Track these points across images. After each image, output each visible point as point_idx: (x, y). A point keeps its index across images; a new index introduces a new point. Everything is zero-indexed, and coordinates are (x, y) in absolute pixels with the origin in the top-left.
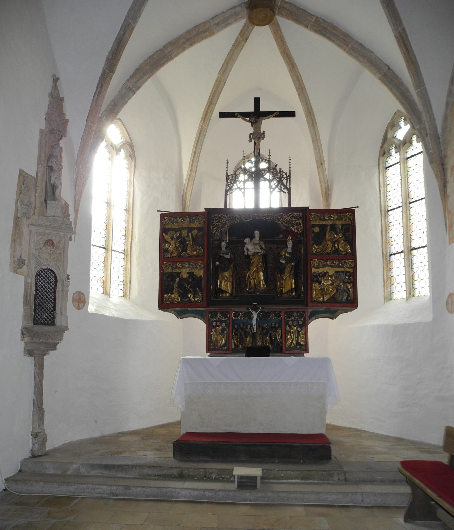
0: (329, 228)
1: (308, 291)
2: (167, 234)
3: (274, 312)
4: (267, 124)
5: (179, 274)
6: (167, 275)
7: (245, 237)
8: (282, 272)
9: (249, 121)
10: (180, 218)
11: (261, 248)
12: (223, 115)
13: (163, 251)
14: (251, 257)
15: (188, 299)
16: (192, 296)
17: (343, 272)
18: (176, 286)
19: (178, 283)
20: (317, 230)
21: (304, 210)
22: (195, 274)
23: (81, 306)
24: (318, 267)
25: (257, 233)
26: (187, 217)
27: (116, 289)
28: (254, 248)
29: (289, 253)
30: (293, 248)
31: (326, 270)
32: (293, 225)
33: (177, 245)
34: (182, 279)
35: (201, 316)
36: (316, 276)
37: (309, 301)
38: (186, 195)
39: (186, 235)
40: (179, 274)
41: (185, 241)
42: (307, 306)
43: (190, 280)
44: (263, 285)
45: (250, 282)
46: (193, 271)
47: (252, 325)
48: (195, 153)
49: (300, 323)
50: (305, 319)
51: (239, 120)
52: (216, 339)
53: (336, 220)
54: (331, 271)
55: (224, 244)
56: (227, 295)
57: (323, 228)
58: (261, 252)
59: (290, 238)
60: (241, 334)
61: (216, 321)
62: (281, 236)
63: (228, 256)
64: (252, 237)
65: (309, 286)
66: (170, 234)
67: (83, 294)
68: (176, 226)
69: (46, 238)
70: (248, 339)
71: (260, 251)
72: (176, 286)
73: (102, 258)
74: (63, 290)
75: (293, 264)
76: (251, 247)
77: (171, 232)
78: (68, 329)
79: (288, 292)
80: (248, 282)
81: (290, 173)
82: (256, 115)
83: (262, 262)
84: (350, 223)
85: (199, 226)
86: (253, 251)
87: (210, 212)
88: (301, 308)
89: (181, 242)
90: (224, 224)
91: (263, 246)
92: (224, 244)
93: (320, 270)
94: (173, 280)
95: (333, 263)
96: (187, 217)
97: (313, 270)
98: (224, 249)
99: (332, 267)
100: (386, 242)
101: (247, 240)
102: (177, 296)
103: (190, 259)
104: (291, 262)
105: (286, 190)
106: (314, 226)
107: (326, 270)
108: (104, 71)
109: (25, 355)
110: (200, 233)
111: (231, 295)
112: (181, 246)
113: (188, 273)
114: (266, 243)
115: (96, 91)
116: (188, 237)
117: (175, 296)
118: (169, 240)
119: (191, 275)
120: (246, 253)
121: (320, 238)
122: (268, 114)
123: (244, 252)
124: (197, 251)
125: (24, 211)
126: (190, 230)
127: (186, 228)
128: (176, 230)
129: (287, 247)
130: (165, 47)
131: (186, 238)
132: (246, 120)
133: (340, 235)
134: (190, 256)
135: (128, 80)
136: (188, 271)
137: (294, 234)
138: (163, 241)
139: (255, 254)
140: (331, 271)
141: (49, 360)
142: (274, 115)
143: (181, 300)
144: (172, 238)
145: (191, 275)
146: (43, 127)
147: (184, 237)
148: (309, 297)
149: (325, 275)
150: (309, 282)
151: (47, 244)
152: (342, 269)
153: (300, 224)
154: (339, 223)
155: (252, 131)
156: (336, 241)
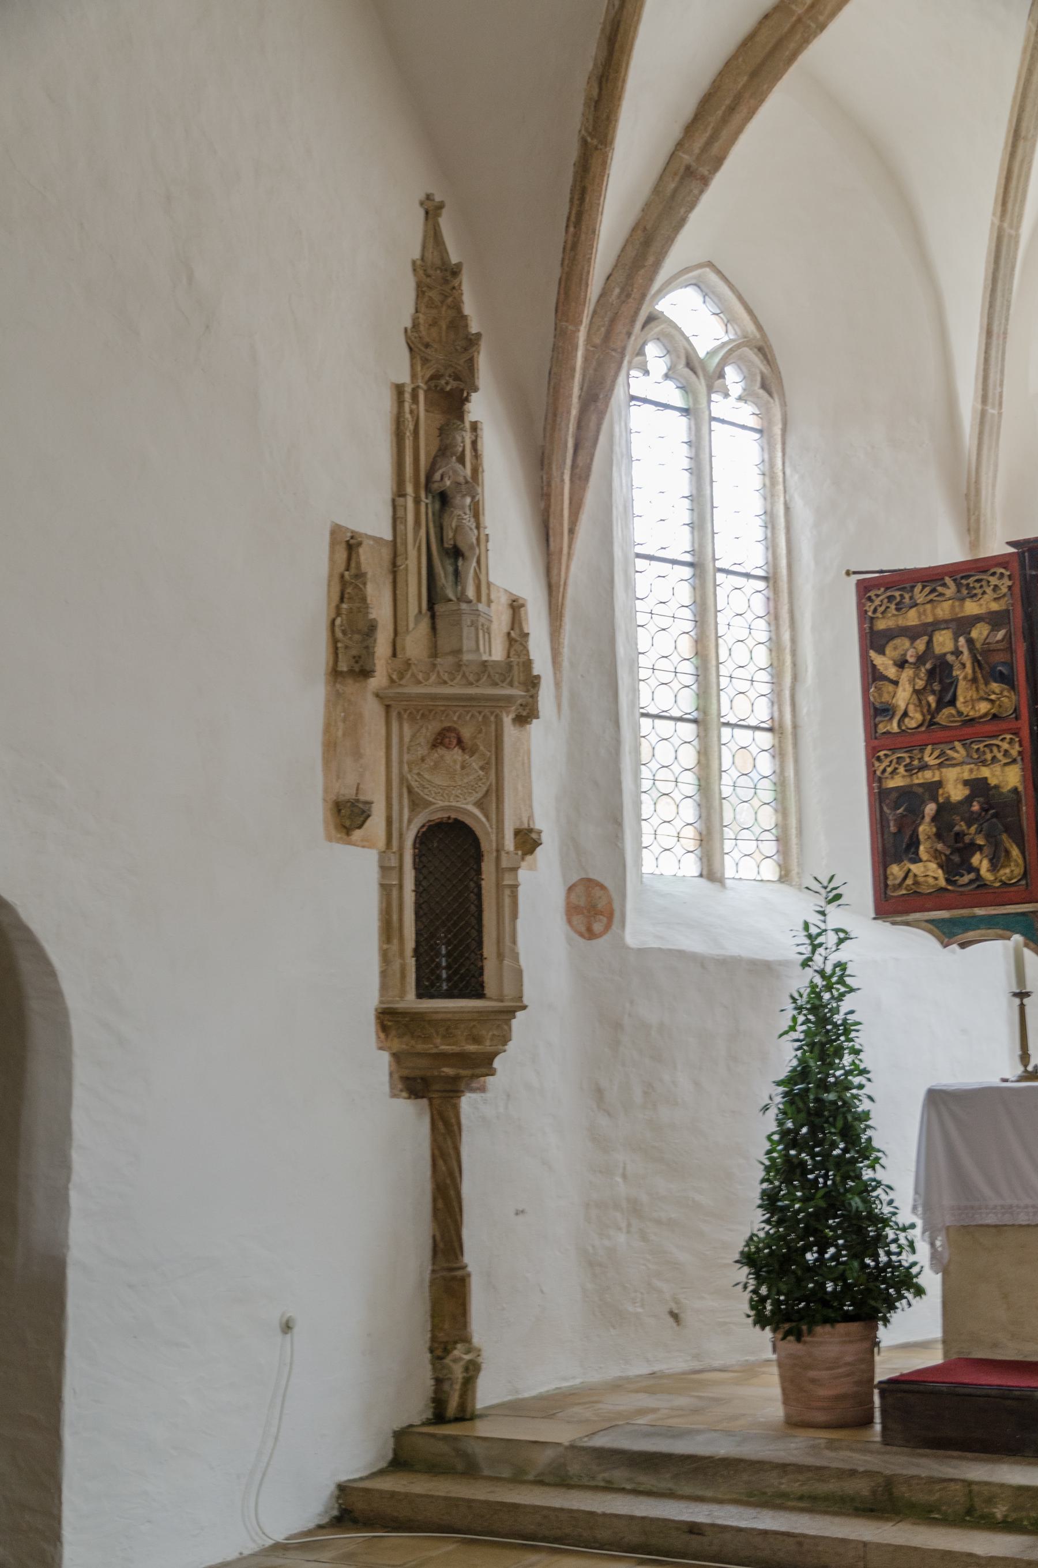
2: (881, 651)
5: (933, 789)
6: (894, 795)
10: (924, 587)
13: (876, 712)
15: (972, 876)
16: (985, 865)
18: (925, 829)
19: (934, 819)
22: (993, 782)
23: (597, 927)
26: (947, 580)
27: (749, 861)
34: (945, 809)
38: (978, 491)
40: (933, 789)
41: (950, 667)
43: (976, 807)
46: (985, 772)
48: (989, 333)
66: (895, 648)
67: (603, 887)
68: (912, 618)
69: (433, 727)
72: (925, 829)
73: (689, 756)
77: (897, 641)
78: (524, 1008)
85: (995, 607)
89: (931, 673)
94: (915, 814)
96: (947, 580)
102: (933, 866)
108: (584, 143)
109: (394, 1096)
110: (1000, 635)
112: (936, 687)
113: (966, 783)
115: (570, 213)
116: (957, 653)
117: (928, 871)
118: (891, 672)
119: (978, 787)
124: (992, 701)
125: (354, 652)
126: (962, 626)
127: (946, 621)
128: (912, 633)
131: (950, 658)
134: (971, 721)
135: (680, 145)
136: (966, 776)
138: (871, 676)
141: (468, 1103)
143: (947, 880)
144: (901, 664)
145: (978, 787)
146: (404, 377)
147: (945, 654)
151: (441, 743)
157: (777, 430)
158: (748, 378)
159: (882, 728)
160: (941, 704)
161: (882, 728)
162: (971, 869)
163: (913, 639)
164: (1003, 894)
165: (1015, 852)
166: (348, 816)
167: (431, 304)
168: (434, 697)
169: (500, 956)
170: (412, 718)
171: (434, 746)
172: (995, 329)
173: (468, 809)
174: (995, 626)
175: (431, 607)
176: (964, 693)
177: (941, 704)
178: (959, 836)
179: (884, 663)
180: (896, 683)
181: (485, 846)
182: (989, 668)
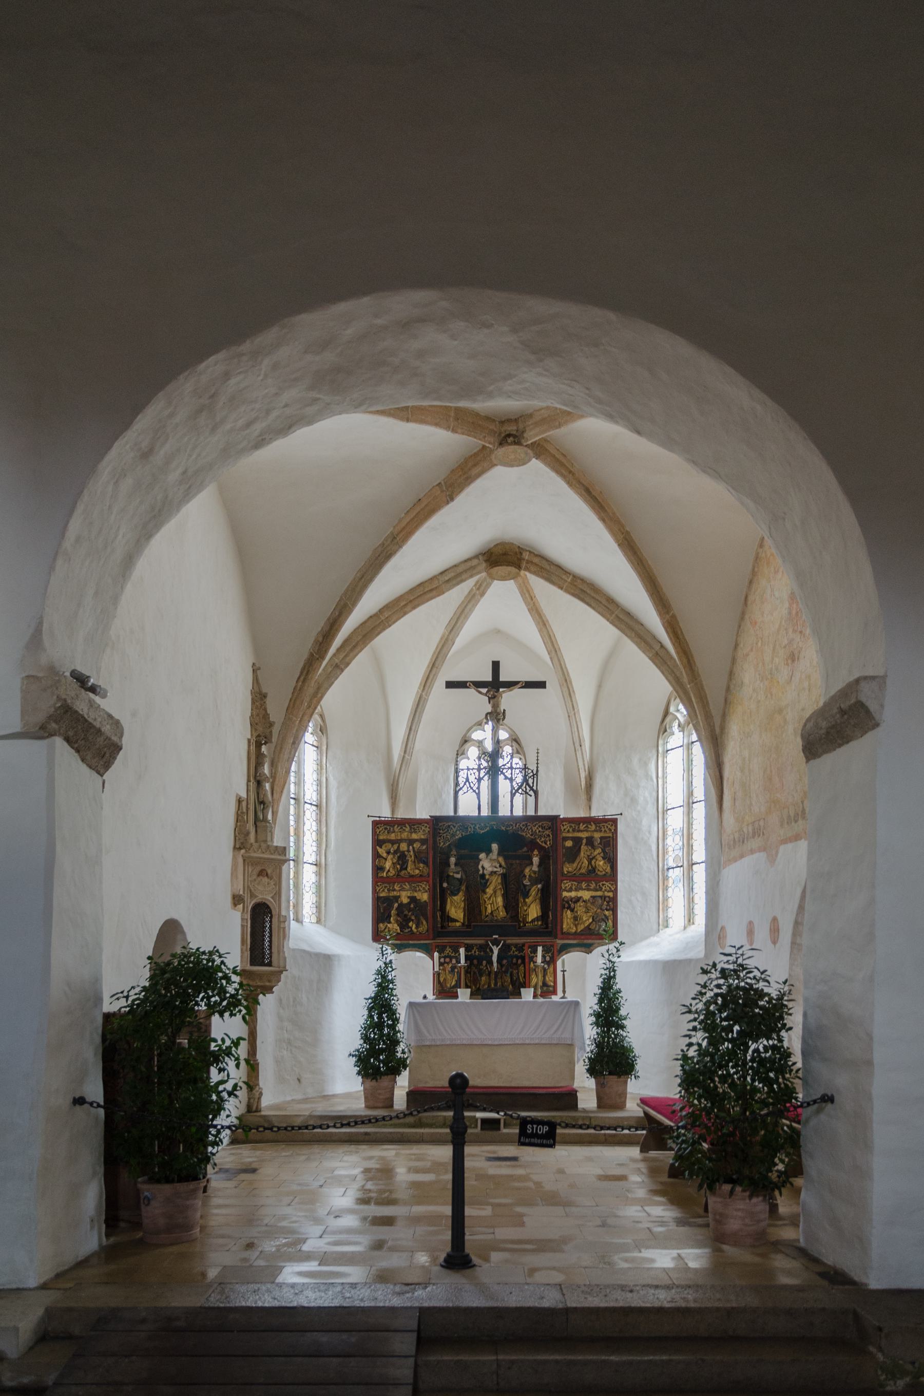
0: (584, 841)
1: (558, 921)
3: (516, 945)
4: (508, 699)
5: (397, 898)
7: (482, 851)
8: (526, 895)
9: (486, 695)
11: (500, 866)
12: (450, 685)
13: (377, 869)
14: (487, 877)
16: (414, 926)
17: (601, 897)
20: (569, 844)
21: (553, 820)
24: (570, 890)
25: (495, 847)
28: (492, 866)
29: (535, 872)
30: (539, 866)
31: (580, 894)
32: (540, 836)
33: (395, 861)
34: (401, 905)
35: (429, 951)
36: (567, 902)
37: (559, 933)
39: (406, 849)
40: (397, 898)
42: (556, 937)
43: (412, 906)
44: (502, 913)
45: (486, 908)
46: (416, 894)
47: (491, 963)
48: (410, 729)
49: (548, 959)
50: (553, 954)
51: (472, 691)
52: (445, 980)
53: (596, 831)
54: (586, 895)
55: (453, 860)
56: (458, 924)
57: (577, 841)
58: (500, 871)
59: (536, 852)
60: (475, 973)
61: (445, 957)
62: (525, 849)
63: (459, 876)
64: (489, 851)
65: (559, 915)
68: (393, 836)
70: (483, 978)
71: (499, 869)
74: (279, 927)
75: (539, 886)
76: (489, 863)
79: (533, 921)
80: (483, 909)
81: (537, 771)
82: (495, 685)
83: (502, 883)
84: (611, 835)
85: (423, 837)
86: (490, 869)
87: (436, 823)
88: (547, 940)
89: (399, 857)
90: (453, 835)
91: (503, 864)
92: (453, 860)
93: (573, 894)
94: (390, 906)
95: (588, 885)
97: (565, 894)
98: (453, 866)
99: (588, 890)
100: (661, 852)
101: (482, 856)
103: (412, 879)
104: (537, 884)
105: (531, 793)
106: (565, 839)
107: (580, 894)
110: (424, 847)
111: (463, 924)
114: (505, 859)
116: (408, 851)
117: (394, 926)
118: (385, 855)
119: (413, 899)
120: (481, 872)
121: (573, 854)
122: (510, 685)
123: (479, 870)
126: (411, 842)
128: (393, 842)
129: (532, 863)
130: (381, 611)
132: (480, 693)
133: (599, 850)
134: (412, 876)
137: (541, 849)
138: (376, 856)
139: (492, 873)
140: (586, 895)
142: (519, 685)
144: (388, 853)
145: (413, 899)
148: (559, 927)
149: (578, 899)
150: (559, 909)
152: (599, 893)
153: (549, 835)
154: (597, 835)
155: (489, 708)
156: (594, 858)
157: (324, 748)
158: (315, 726)
159: (380, 875)
160: (402, 869)
161: (380, 875)
162: (409, 927)
163: (393, 844)
164: (420, 936)
165: (424, 923)
166: (237, 900)
167: (257, 708)
168: (261, 858)
169: (279, 952)
170: (252, 865)
171: (258, 875)
172: (413, 728)
173: (268, 898)
174: (422, 844)
175: (255, 823)
176: (410, 866)
177: (402, 869)
178: (406, 916)
179: (382, 851)
180: (386, 859)
181: (273, 913)
182: (420, 858)
